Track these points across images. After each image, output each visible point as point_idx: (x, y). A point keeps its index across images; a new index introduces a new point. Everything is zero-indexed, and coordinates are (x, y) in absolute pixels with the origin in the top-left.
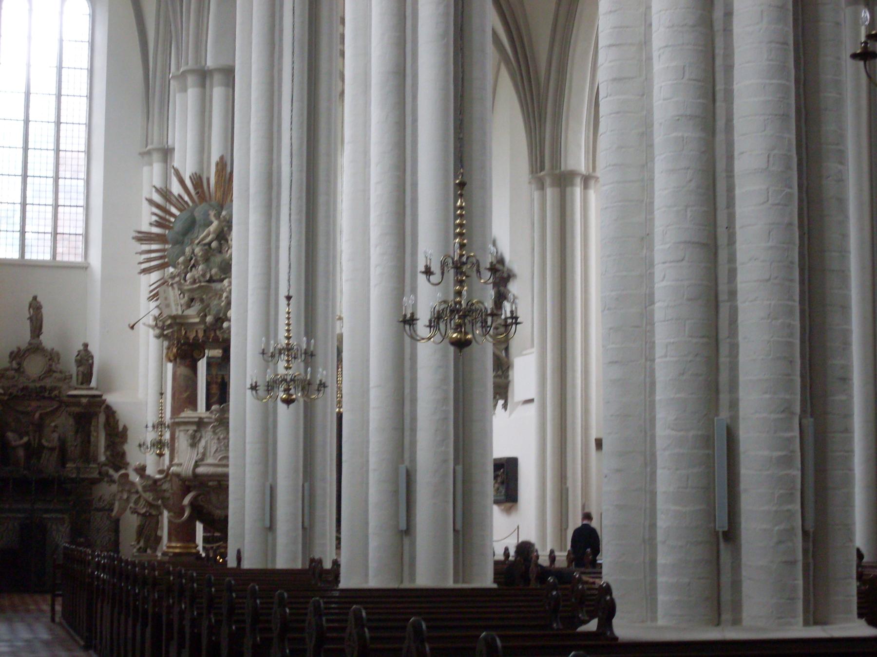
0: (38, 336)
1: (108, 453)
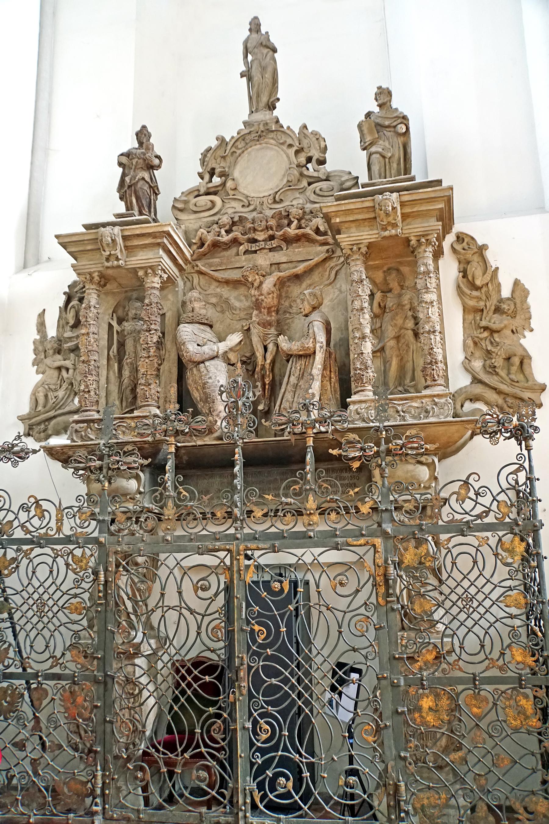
0: (272, 107)
1: (478, 364)
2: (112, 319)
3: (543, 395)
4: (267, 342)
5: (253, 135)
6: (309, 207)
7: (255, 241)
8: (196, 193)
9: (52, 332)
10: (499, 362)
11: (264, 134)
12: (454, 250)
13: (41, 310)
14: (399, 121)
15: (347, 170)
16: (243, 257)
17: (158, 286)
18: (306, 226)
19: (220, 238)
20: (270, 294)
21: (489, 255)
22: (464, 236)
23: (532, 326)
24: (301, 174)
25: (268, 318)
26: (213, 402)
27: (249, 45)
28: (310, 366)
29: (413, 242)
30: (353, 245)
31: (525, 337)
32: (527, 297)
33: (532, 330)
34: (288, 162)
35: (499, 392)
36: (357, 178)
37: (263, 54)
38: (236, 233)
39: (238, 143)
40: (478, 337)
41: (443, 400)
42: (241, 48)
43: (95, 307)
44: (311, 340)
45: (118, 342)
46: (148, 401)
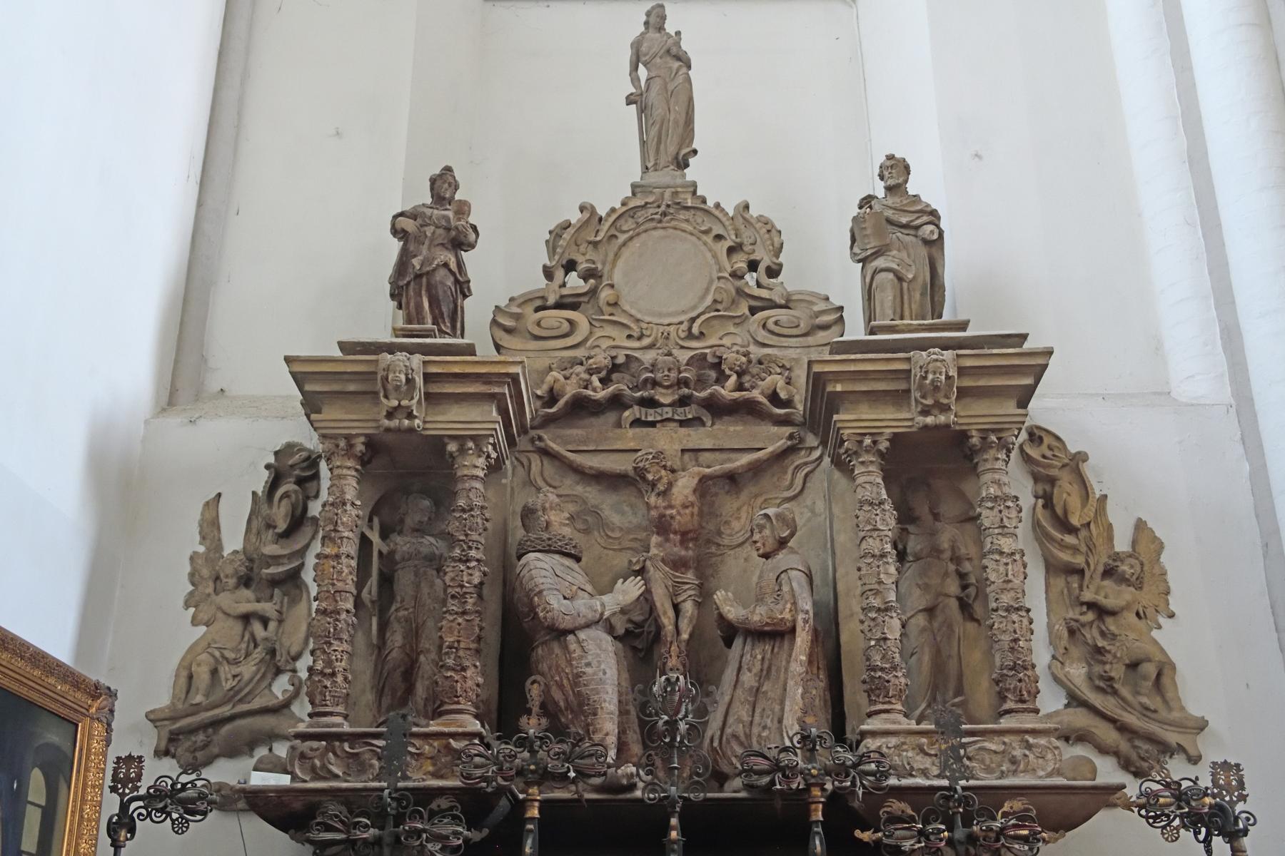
0: (682, 164)
1: (1077, 672)
2: (371, 528)
3: (1200, 739)
4: (680, 599)
5: (652, 211)
6: (756, 352)
7: (650, 403)
8: (538, 303)
9: (233, 540)
10: (1117, 671)
11: (671, 211)
12: (1027, 458)
13: (213, 495)
14: (925, 218)
15: (823, 292)
16: (631, 432)
17: (481, 474)
18: (753, 387)
19: (589, 392)
20: (687, 507)
21: (1088, 470)
22: (1043, 434)
23: (1172, 607)
24: (740, 292)
25: (683, 553)
26: (595, 714)
27: (644, 49)
28: (785, 656)
29: (975, 441)
30: (865, 434)
31: (1159, 627)
32: (1159, 554)
33: (1172, 616)
34: (715, 267)
35: (1122, 728)
36: (841, 309)
37: (670, 68)
38: (620, 385)
39: (622, 221)
40: (1077, 621)
41: (1042, 741)
42: (627, 55)
43: (353, 504)
44: (789, 606)
45: (381, 573)
46: (458, 703)
